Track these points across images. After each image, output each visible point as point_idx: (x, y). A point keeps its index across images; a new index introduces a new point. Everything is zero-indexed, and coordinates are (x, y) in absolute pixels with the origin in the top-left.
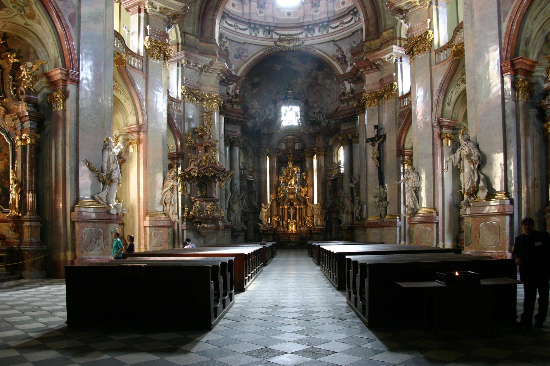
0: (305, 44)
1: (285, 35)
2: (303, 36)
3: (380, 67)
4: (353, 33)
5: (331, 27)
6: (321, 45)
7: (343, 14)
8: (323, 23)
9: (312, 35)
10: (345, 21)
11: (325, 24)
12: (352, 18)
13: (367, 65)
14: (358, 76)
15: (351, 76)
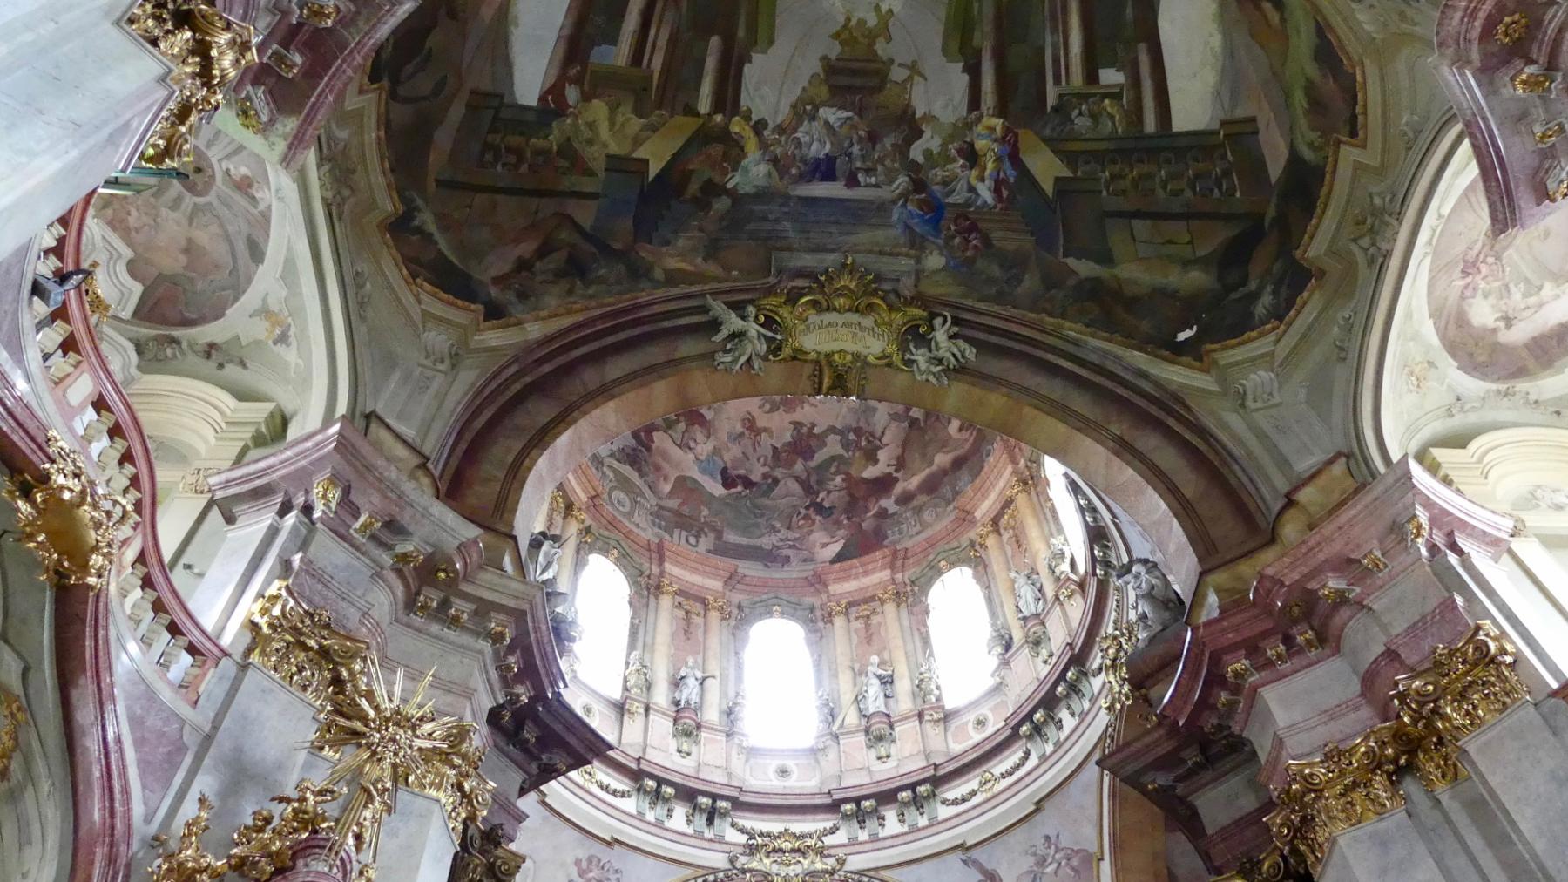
0: (848, 867)
1: (768, 835)
2: (841, 837)
3: (1344, 613)
4: (1039, 806)
5: (943, 802)
6: (914, 867)
7: (987, 747)
8: (912, 787)
9: (874, 838)
10: (997, 771)
11: (921, 789)
12: (1027, 754)
13: (1268, 624)
14: (1210, 722)
15: (1168, 746)
